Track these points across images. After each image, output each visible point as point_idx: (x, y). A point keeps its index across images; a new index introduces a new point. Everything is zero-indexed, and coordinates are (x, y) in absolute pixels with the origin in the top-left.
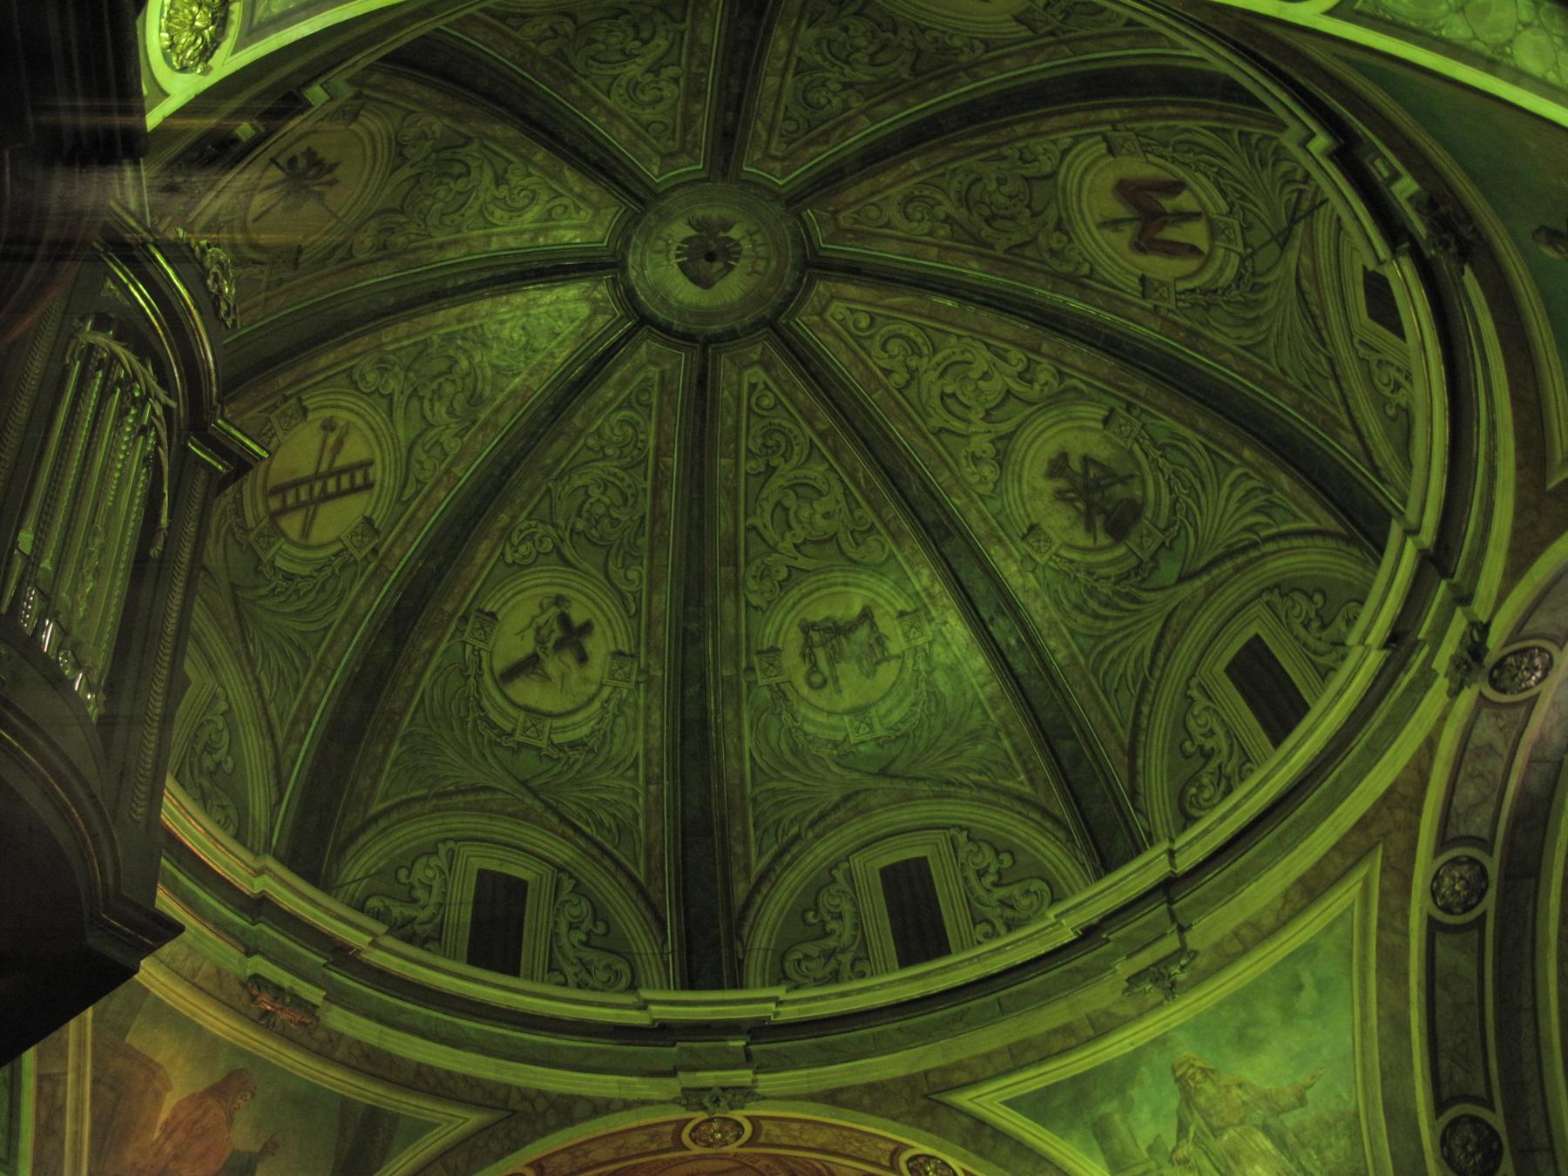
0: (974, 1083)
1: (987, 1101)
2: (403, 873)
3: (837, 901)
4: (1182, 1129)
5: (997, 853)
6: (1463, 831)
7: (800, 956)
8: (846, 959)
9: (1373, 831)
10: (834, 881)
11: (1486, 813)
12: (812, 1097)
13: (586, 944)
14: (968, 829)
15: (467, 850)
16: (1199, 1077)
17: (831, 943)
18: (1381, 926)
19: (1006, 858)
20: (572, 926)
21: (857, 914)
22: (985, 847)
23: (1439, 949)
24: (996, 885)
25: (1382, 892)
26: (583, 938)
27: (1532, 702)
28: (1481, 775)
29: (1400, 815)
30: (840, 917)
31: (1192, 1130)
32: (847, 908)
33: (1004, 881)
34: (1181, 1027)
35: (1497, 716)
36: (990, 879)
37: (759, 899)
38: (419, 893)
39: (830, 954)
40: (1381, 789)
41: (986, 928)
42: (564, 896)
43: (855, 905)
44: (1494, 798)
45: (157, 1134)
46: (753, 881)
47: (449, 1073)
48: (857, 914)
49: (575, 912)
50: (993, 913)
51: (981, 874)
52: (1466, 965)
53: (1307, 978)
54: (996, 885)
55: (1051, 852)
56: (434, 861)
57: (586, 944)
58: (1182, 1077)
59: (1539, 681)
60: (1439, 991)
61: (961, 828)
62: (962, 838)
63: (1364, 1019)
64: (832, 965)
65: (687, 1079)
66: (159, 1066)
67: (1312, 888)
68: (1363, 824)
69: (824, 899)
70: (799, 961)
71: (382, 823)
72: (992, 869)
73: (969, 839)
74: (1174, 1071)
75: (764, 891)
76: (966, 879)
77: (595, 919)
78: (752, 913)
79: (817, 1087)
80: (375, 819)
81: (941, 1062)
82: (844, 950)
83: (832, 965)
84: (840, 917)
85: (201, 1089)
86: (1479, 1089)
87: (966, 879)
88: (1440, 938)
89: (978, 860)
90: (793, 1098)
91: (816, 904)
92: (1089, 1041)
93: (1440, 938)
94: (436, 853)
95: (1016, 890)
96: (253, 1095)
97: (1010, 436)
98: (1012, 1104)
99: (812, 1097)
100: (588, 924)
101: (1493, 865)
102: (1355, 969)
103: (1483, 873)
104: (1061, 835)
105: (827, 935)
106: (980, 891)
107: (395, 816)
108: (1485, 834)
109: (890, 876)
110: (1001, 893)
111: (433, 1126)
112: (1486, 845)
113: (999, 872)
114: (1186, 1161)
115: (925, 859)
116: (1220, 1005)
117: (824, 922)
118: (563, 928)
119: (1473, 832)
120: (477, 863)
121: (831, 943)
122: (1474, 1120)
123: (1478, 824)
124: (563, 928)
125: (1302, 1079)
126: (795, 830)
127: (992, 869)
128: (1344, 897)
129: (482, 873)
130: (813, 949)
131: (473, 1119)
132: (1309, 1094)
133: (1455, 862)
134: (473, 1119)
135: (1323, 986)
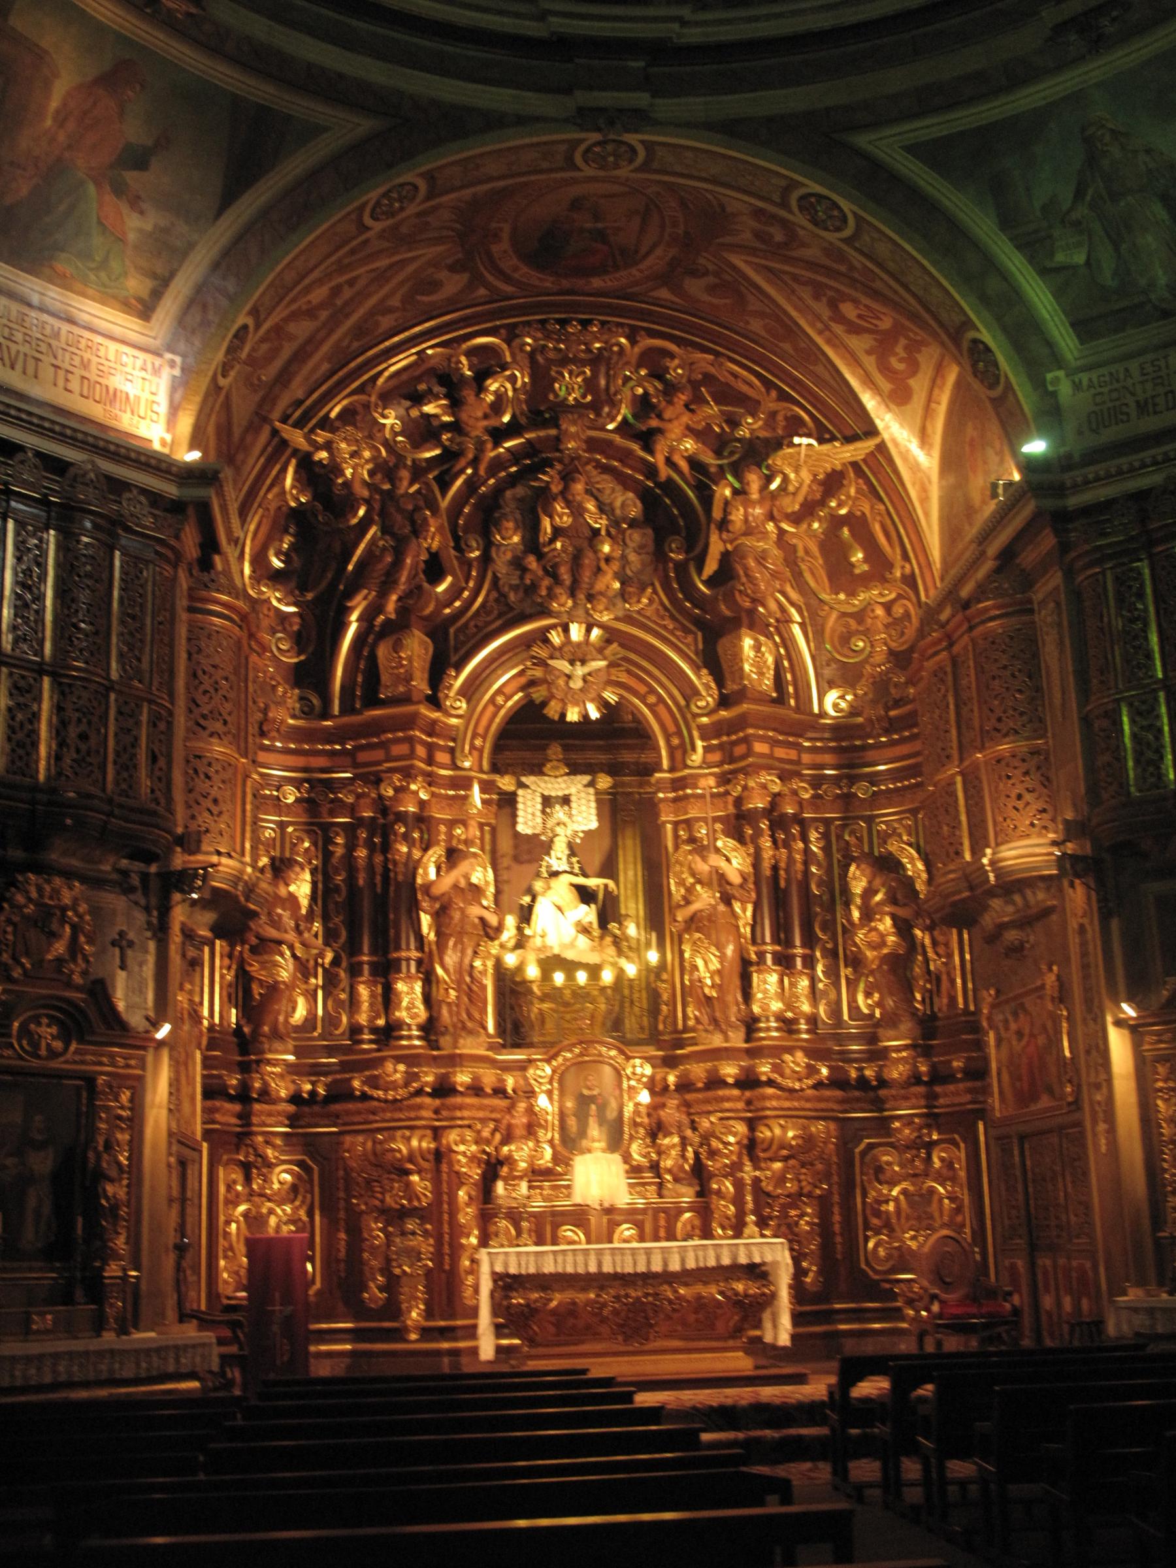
1: (887, 145)
4: (1079, 194)
16: (1107, 138)
31: (1090, 192)
47: (341, 76)
65: (581, 98)
66: (46, 52)
74: (1083, 129)
90: (688, 125)
98: (913, 149)
111: (326, 129)
114: (1077, 224)
131: (364, 125)
134: (364, 125)
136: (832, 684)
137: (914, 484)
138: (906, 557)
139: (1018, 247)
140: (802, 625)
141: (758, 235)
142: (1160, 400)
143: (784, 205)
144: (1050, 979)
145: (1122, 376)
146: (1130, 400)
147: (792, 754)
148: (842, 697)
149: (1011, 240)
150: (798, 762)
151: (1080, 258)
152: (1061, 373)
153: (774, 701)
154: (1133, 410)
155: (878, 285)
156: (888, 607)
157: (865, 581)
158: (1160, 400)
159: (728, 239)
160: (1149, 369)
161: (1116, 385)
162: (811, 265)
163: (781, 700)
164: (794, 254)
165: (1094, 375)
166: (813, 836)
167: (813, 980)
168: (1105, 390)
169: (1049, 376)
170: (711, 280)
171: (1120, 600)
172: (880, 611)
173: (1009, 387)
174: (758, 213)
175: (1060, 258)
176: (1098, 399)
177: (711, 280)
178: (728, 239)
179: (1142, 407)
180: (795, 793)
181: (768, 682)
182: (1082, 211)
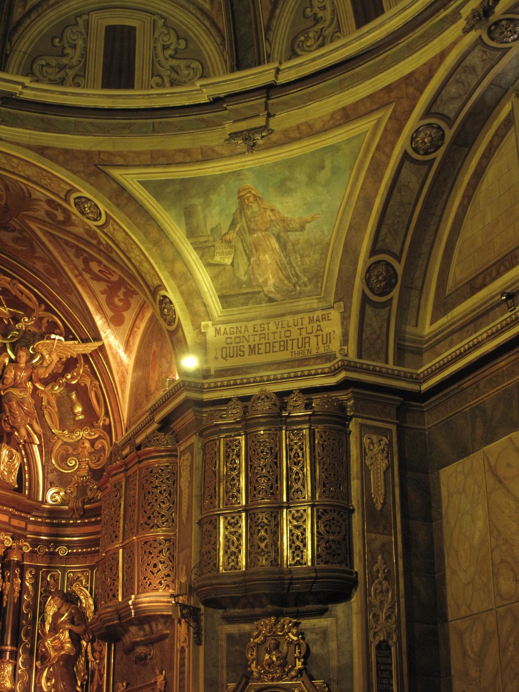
0: (126, 166)
1: (130, 178)
3: (75, 37)
4: (233, 225)
5: (178, 38)
6: (440, 110)
7: (44, 63)
8: (71, 73)
9: (394, 94)
10: (77, 24)
11: (457, 104)
12: (30, 147)
14: (166, 19)
16: (251, 199)
17: (65, 61)
18: (378, 148)
21: (85, 48)
22: (172, 32)
23: (404, 170)
24: (172, 57)
25: (385, 130)
27: (506, 51)
28: (463, 83)
29: (411, 90)
31: (239, 226)
32: (80, 43)
33: (177, 56)
34: (250, 169)
35: (484, 52)
36: (170, 52)
37: (28, 21)
39: (63, 67)
40: (406, 72)
41: (158, 80)
43: (85, 42)
44: (465, 97)
46: (28, 8)
48: (85, 48)
50: (166, 73)
51: (165, 48)
52: (414, 184)
53: (328, 164)
54: (172, 57)
55: (210, 48)
58: (242, 196)
59: (514, 40)
60: (395, 192)
61: (162, 17)
63: (351, 195)
64: (62, 74)
68: (388, 89)
69: (68, 34)
70: (43, 66)
72: (173, 47)
73: (164, 25)
74: (239, 192)
75: (33, 17)
76: (155, 47)
78: (22, 28)
79: (33, 142)
81: (110, 149)
82: (72, 67)
83: (62, 74)
84: (74, 47)
86: (396, 250)
87: (155, 47)
88: (407, 164)
89: (166, 39)
90: (18, 144)
91: (62, 34)
92: (198, 162)
93: (407, 164)
95: (182, 64)
98: (143, 183)
99: (30, 147)
101: (449, 134)
102: (355, 167)
103: (443, 136)
104: (219, 40)
105: (63, 55)
106: (161, 58)
108: (452, 115)
109: (110, 30)
110: (173, 62)
112: (450, 122)
113: (176, 50)
114: (230, 242)
115: (134, 28)
116: (276, 164)
117: (64, 47)
119: (446, 112)
121: (65, 61)
122: (388, 264)
123: (450, 109)
125: (306, 217)
127: (173, 47)
128: (365, 125)
130: (53, 61)
132: (308, 226)
133: (430, 125)
135: (335, 170)
136: (52, 484)
137: (118, 373)
138: (107, 414)
139: (195, 249)
140: (40, 446)
141: (48, 213)
142: (262, 347)
143: (66, 200)
144: (160, 679)
145: (243, 330)
146: (246, 344)
147: (22, 524)
148: (58, 493)
149: (191, 244)
150: (25, 529)
151: (228, 261)
152: (210, 323)
153: (15, 490)
154: (247, 350)
155: (113, 255)
156: (92, 442)
157: (81, 425)
158: (262, 347)
159: (30, 213)
160: (258, 328)
161: (239, 335)
162: (77, 237)
163: (20, 490)
164: (68, 229)
165: (228, 327)
166: (28, 576)
167: (15, 668)
168: (233, 336)
169: (203, 323)
170: (16, 234)
171: (227, 456)
172: (87, 444)
173: (179, 326)
174: (50, 202)
175: (218, 259)
176: (229, 341)
177: (16, 234)
178: (30, 213)
179: (252, 350)
180: (21, 548)
181: (13, 479)
182: (232, 236)
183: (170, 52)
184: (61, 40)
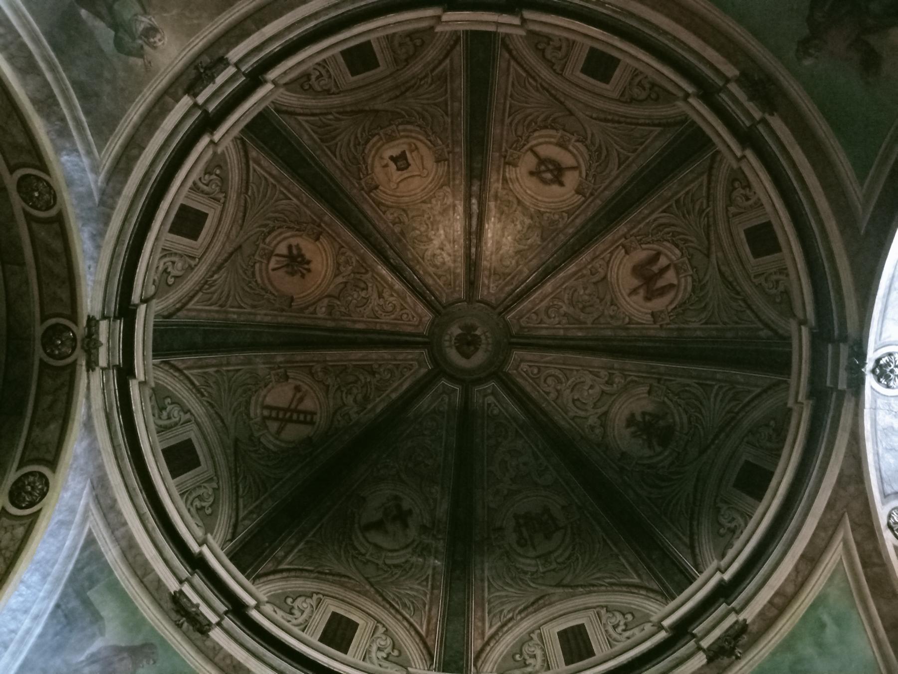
2: (289, 601)
3: (533, 649)
5: (624, 615)
9: (839, 506)
10: (532, 639)
13: (386, 659)
14: (606, 607)
15: (328, 601)
18: (864, 565)
19: (629, 617)
20: (379, 649)
21: (545, 655)
24: (624, 630)
25: (858, 544)
26: (385, 656)
29: (852, 489)
30: (534, 656)
32: (539, 653)
33: (629, 627)
36: (621, 627)
37: (488, 648)
38: (296, 612)
42: (378, 634)
43: (543, 650)
45: (83, 658)
46: (486, 639)
49: (383, 643)
51: (615, 627)
53: (826, 618)
54: (624, 630)
56: (309, 600)
57: (386, 659)
61: (602, 607)
62: (603, 611)
63: (875, 632)
66: (101, 618)
67: (811, 559)
68: (830, 506)
69: (526, 649)
71: (285, 574)
72: (622, 623)
73: (607, 611)
75: (492, 645)
76: (606, 631)
77: (393, 648)
78: (484, 655)
80: (282, 571)
84: (534, 656)
85: (123, 645)
87: (606, 631)
89: (613, 620)
91: (521, 650)
94: (311, 597)
96: (155, 662)
97: (605, 414)
100: (389, 650)
102: (857, 602)
104: (659, 598)
105: (526, 665)
107: (293, 574)
109: (562, 635)
113: (626, 624)
115: (583, 625)
116: (773, 654)
117: (525, 660)
118: (374, 648)
120: (333, 609)
124: (374, 648)
126: (510, 615)
127: (622, 623)
128: (834, 556)
129: (334, 615)
135: (839, 621)
183: (619, 629)
184: (521, 654)
